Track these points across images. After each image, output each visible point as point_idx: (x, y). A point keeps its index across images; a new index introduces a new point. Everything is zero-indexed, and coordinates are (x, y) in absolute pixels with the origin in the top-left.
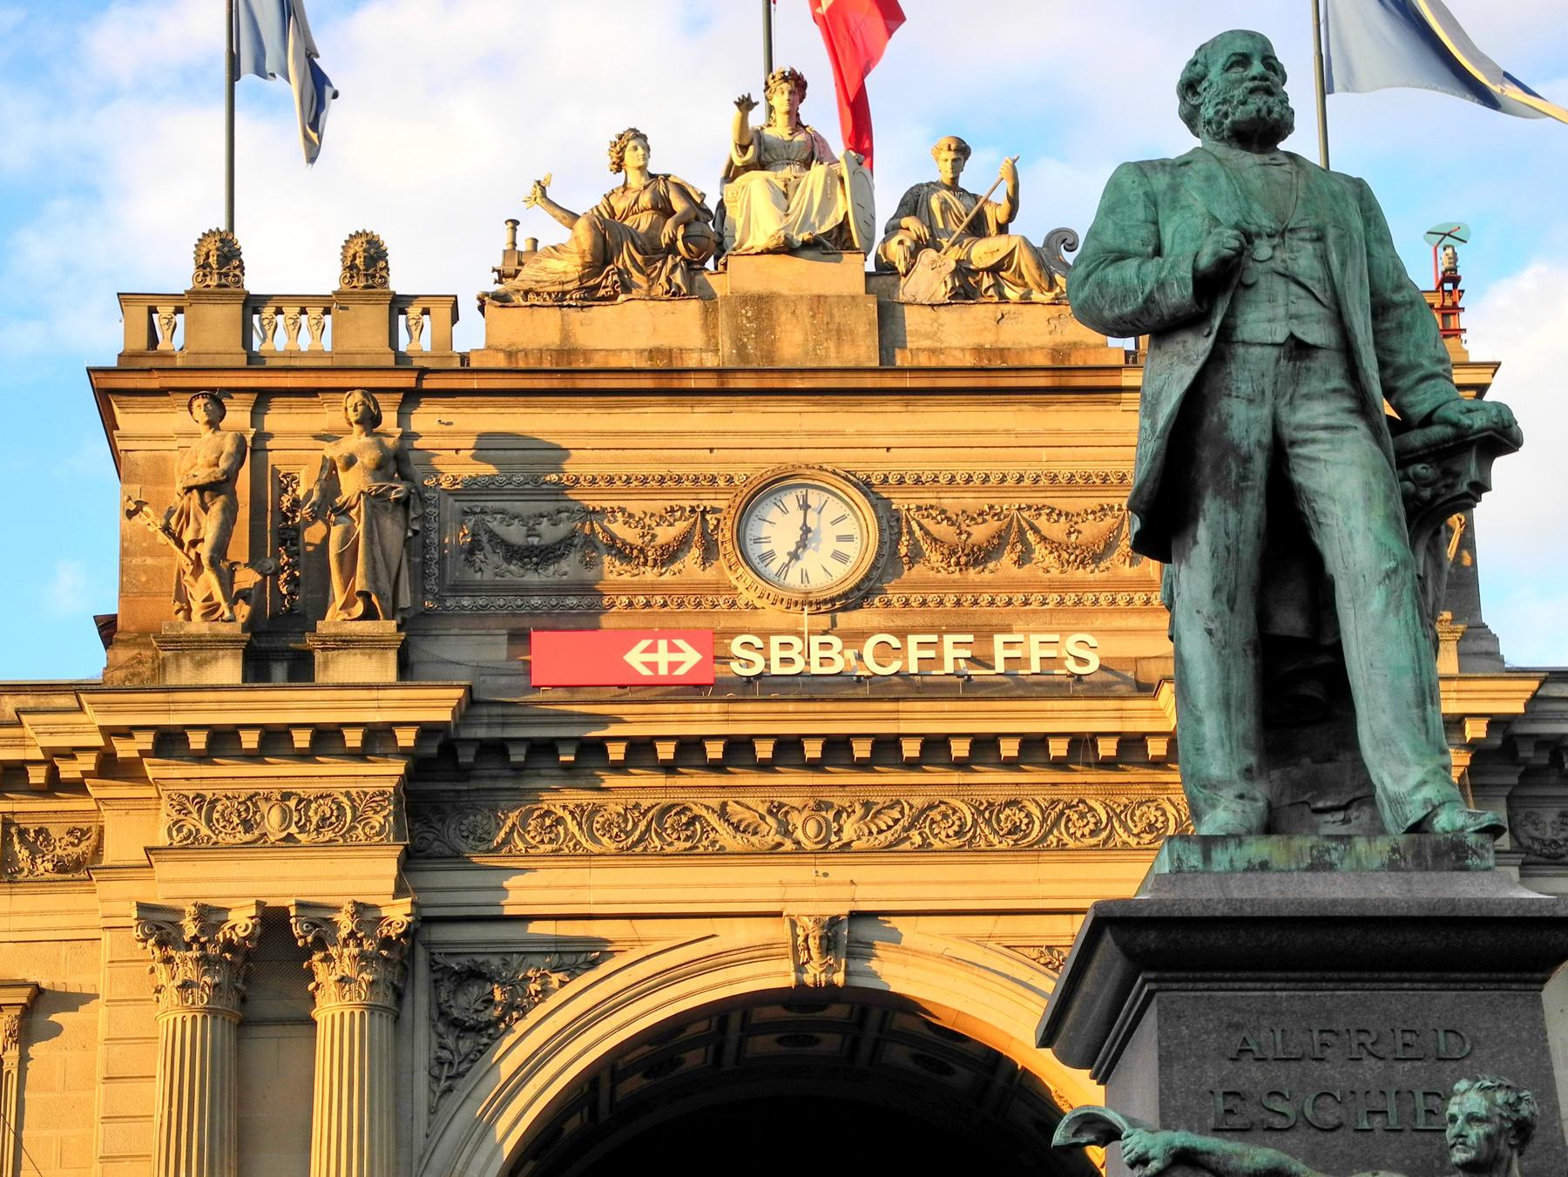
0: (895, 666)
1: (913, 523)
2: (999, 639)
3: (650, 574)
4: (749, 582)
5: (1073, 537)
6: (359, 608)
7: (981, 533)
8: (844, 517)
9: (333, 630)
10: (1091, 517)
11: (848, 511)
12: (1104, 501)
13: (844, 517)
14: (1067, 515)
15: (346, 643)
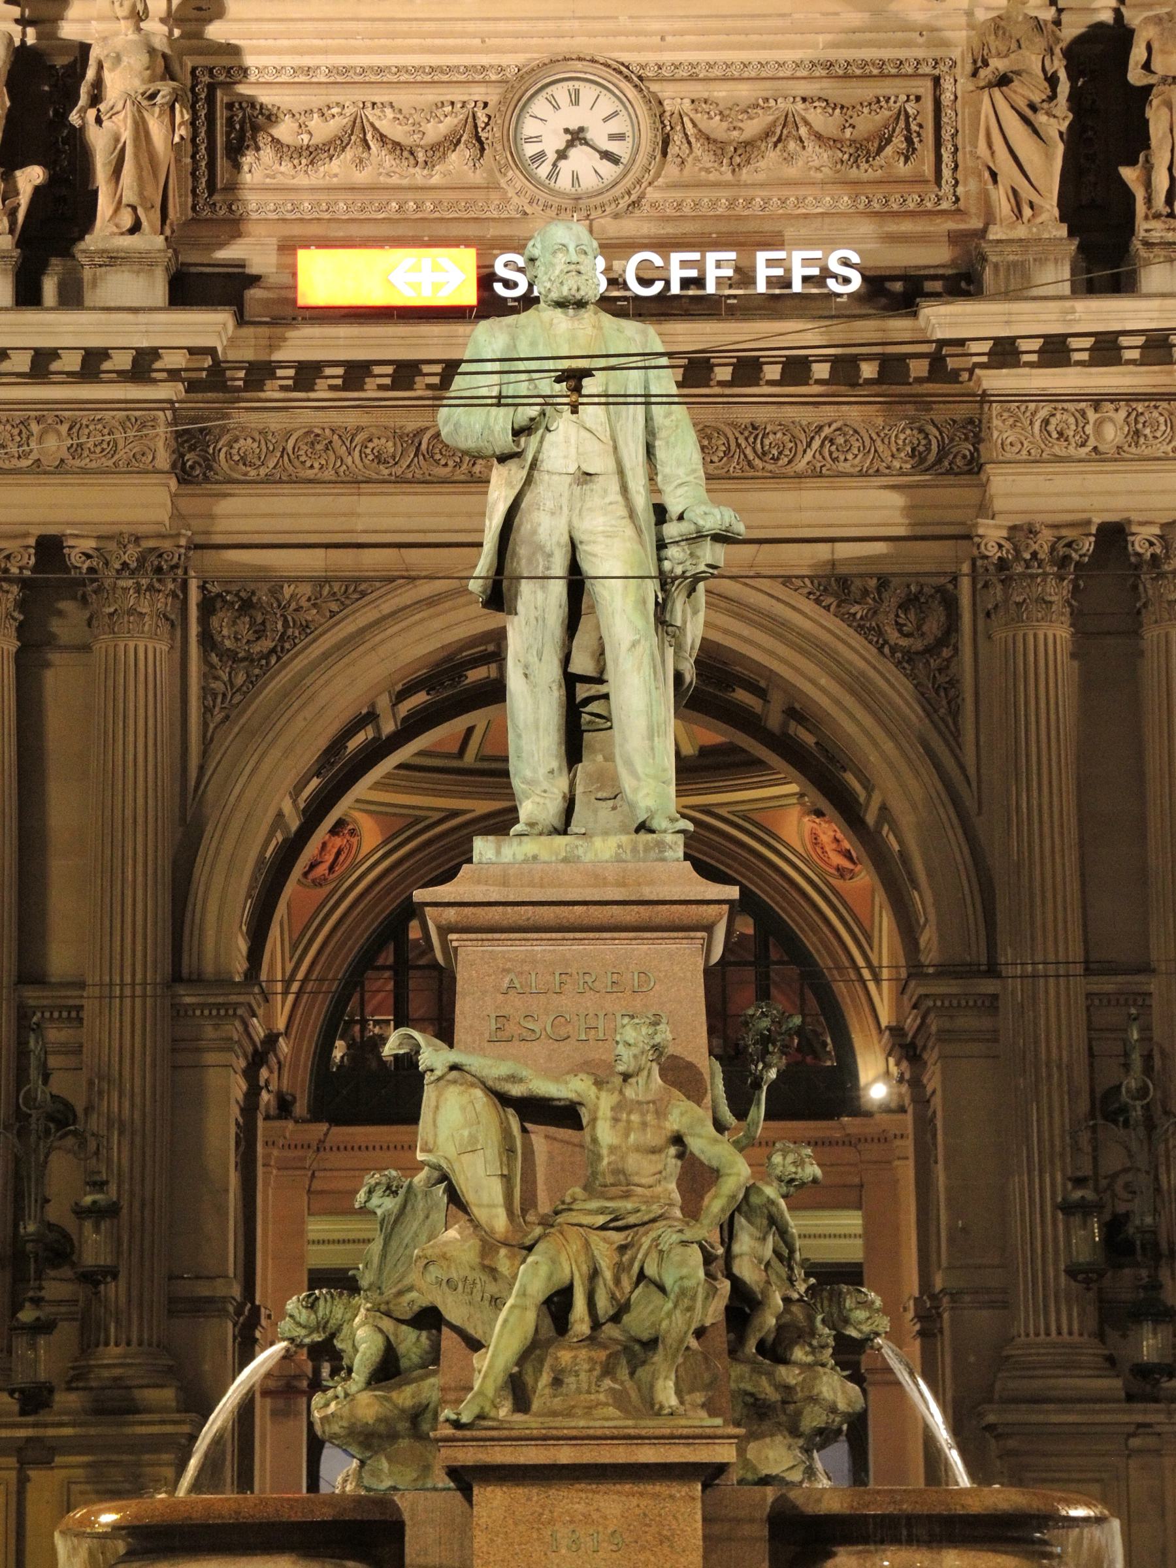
0: (658, 287)
1: (686, 119)
2: (762, 257)
3: (419, 175)
4: (518, 185)
5: (848, 131)
6: (127, 220)
7: (752, 127)
8: (616, 114)
9: (101, 246)
10: (866, 110)
11: (621, 107)
12: (880, 92)
13: (616, 114)
14: (842, 107)
15: (113, 259)
